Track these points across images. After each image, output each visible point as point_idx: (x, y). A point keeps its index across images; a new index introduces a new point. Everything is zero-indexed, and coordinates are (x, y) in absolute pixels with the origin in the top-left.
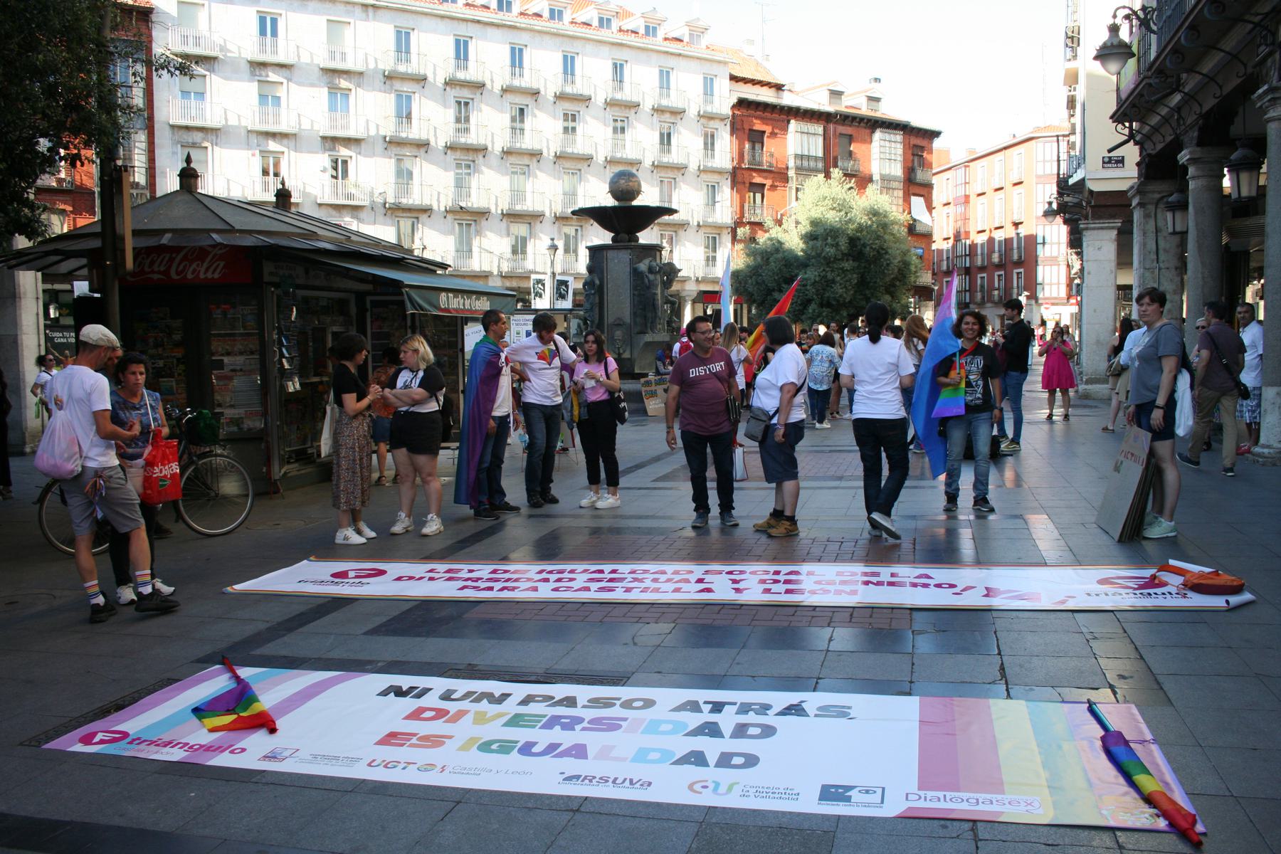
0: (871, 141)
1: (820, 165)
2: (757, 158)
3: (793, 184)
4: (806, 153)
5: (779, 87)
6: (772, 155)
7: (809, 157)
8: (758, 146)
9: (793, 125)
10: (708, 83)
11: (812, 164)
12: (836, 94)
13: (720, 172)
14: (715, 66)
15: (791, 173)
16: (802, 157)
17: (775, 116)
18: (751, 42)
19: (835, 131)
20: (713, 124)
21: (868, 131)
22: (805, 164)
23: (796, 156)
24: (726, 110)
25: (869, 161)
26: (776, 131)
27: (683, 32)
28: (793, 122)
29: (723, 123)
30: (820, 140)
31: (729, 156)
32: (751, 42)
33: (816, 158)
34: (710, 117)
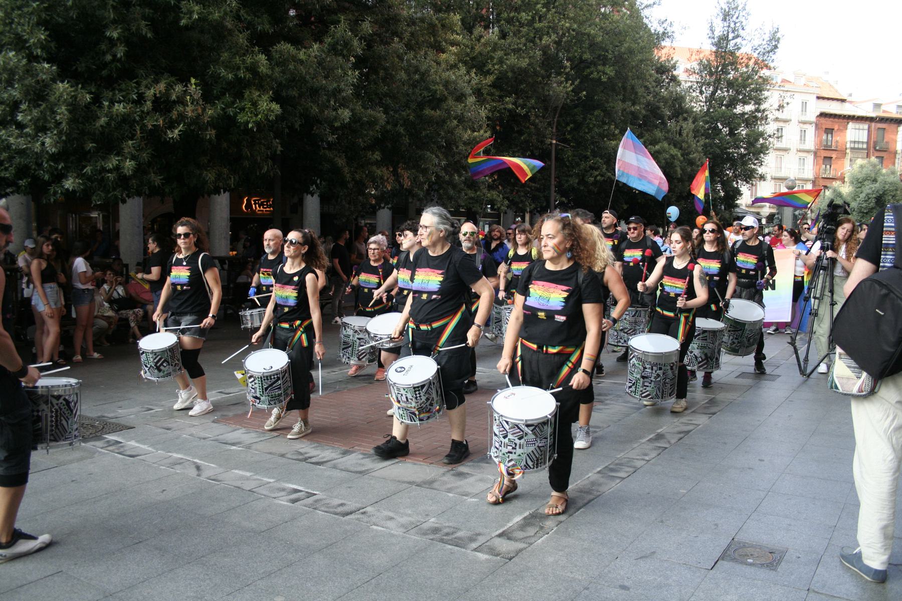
0: (898, 132)
1: (865, 146)
2: (829, 144)
3: (848, 157)
4: (857, 140)
5: (843, 101)
6: (837, 142)
7: (859, 142)
8: (830, 136)
9: (851, 125)
10: (804, 104)
11: (860, 146)
12: (877, 106)
13: (808, 151)
14: (808, 95)
15: (848, 151)
16: (855, 142)
17: (841, 120)
18: (827, 73)
19: (875, 127)
20: (805, 126)
21: (896, 125)
22: (856, 146)
23: (851, 142)
24: (813, 118)
25: (896, 142)
26: (841, 128)
27: (790, 78)
28: (850, 123)
29: (810, 126)
30: (866, 132)
31: (813, 143)
32: (827, 73)
33: (863, 143)
34: (804, 123)
